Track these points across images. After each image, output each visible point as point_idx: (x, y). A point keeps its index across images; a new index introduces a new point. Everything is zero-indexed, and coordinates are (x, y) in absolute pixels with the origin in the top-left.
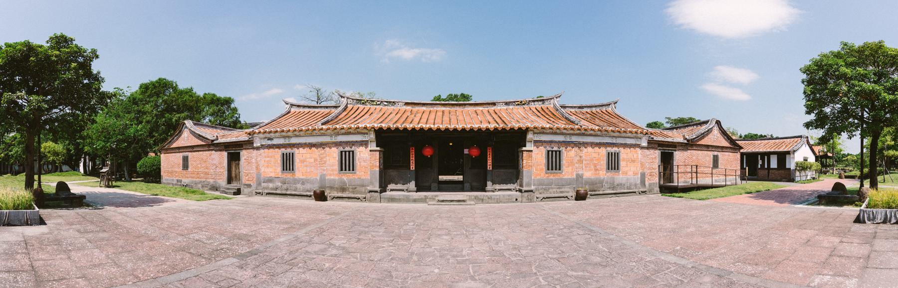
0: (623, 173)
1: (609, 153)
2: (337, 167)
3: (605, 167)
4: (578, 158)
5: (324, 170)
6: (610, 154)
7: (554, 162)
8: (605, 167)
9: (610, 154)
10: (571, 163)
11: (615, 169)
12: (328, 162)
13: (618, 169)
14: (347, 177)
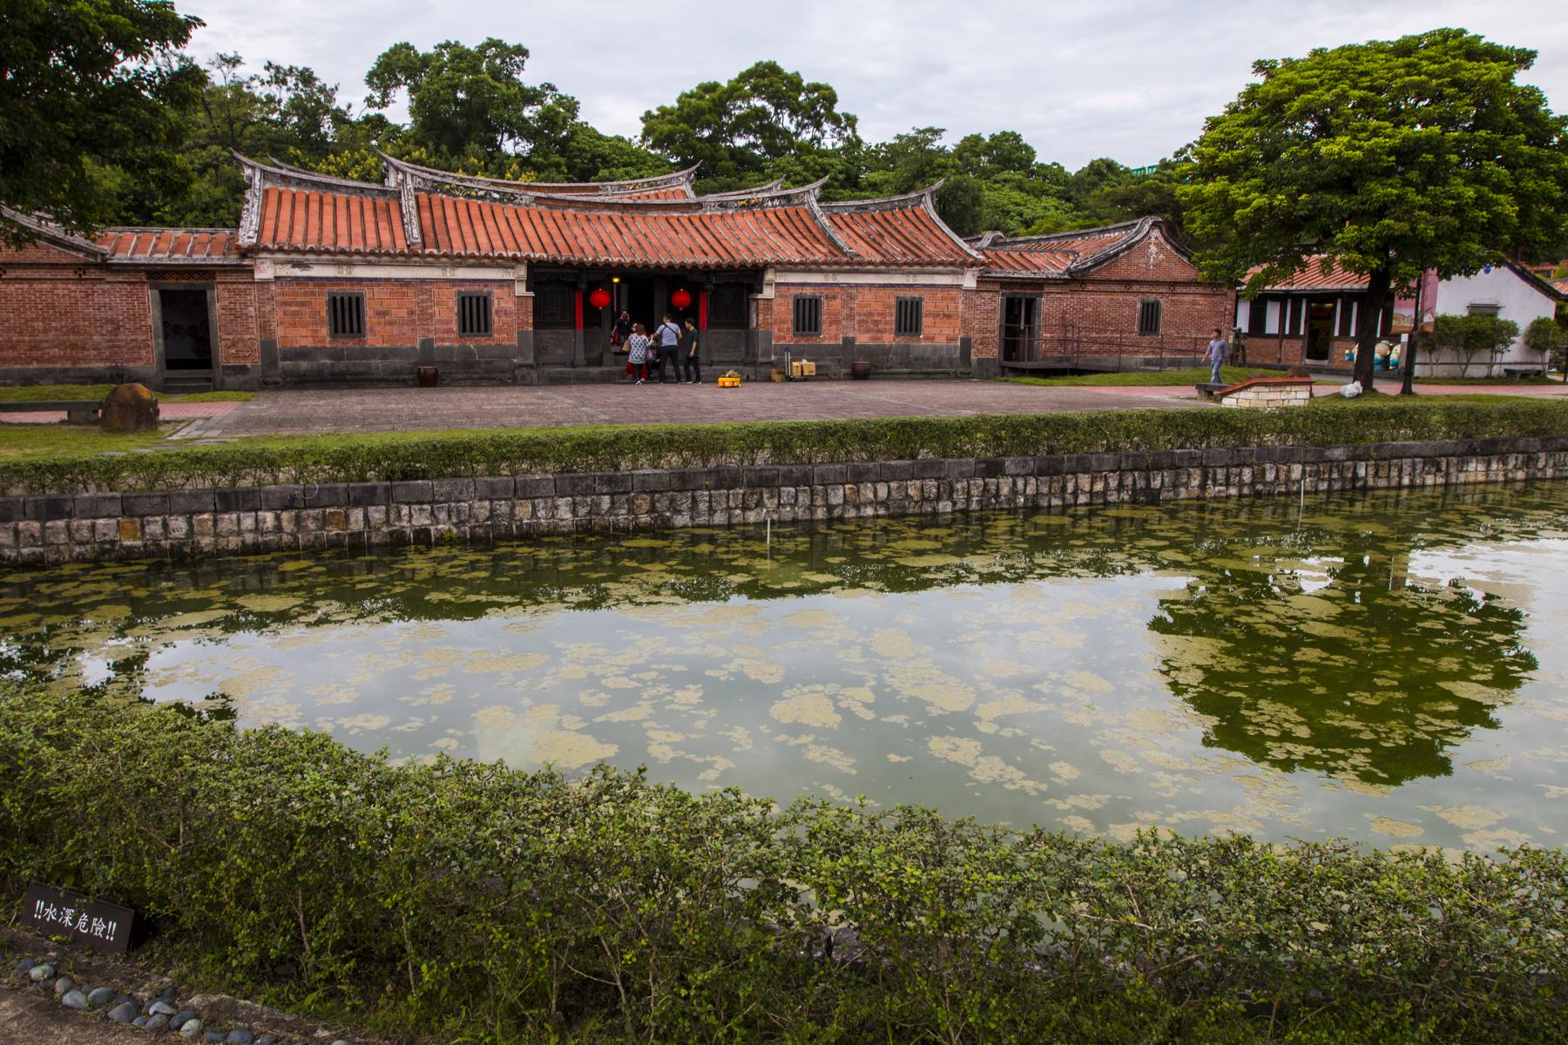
0: (926, 339)
4: (846, 311)
5: (429, 331)
10: (837, 322)
12: (437, 317)
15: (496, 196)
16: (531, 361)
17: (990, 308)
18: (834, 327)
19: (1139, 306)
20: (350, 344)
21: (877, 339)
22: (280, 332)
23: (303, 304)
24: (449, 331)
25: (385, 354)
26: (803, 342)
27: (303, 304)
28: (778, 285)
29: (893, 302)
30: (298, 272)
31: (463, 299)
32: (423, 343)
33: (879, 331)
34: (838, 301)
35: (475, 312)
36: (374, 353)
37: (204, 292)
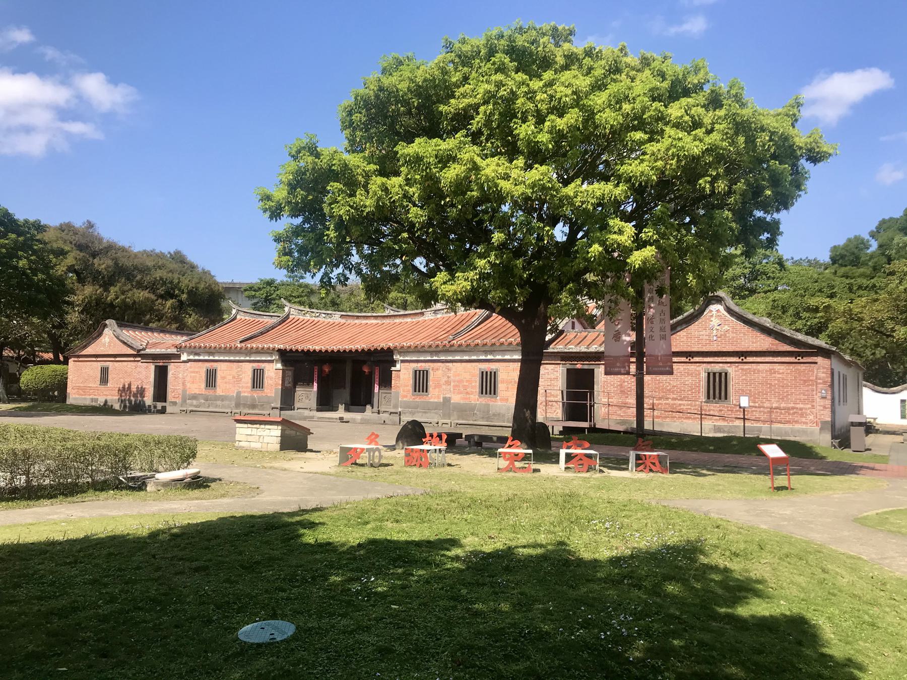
0: (501, 400)
1: (483, 372)
2: (250, 384)
3: (478, 389)
4: (445, 379)
5: (239, 387)
6: (484, 373)
7: (421, 382)
8: (478, 390)
9: (484, 373)
10: (438, 386)
11: (490, 394)
12: (243, 380)
13: (495, 394)
14: (257, 394)
15: (324, 315)
16: (279, 406)
17: (553, 377)
18: (437, 390)
19: (704, 375)
20: (210, 392)
21: (466, 399)
22: (188, 385)
23: (197, 372)
24: (247, 387)
25: (223, 398)
26: (417, 400)
27: (197, 372)
28: (403, 361)
29: (478, 373)
30: (197, 358)
31: (254, 370)
32: (237, 393)
33: (467, 393)
34: (440, 371)
35: (258, 380)
36: (217, 398)
37: (167, 366)
